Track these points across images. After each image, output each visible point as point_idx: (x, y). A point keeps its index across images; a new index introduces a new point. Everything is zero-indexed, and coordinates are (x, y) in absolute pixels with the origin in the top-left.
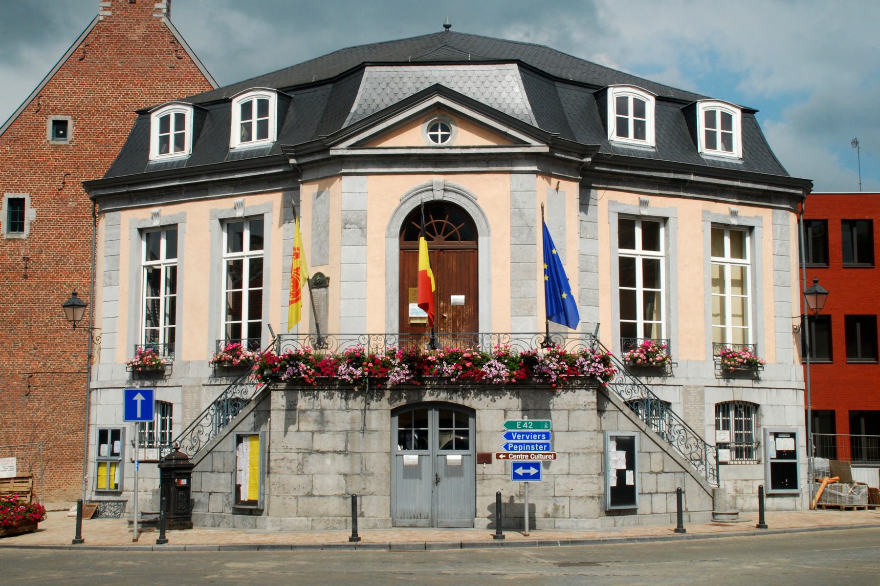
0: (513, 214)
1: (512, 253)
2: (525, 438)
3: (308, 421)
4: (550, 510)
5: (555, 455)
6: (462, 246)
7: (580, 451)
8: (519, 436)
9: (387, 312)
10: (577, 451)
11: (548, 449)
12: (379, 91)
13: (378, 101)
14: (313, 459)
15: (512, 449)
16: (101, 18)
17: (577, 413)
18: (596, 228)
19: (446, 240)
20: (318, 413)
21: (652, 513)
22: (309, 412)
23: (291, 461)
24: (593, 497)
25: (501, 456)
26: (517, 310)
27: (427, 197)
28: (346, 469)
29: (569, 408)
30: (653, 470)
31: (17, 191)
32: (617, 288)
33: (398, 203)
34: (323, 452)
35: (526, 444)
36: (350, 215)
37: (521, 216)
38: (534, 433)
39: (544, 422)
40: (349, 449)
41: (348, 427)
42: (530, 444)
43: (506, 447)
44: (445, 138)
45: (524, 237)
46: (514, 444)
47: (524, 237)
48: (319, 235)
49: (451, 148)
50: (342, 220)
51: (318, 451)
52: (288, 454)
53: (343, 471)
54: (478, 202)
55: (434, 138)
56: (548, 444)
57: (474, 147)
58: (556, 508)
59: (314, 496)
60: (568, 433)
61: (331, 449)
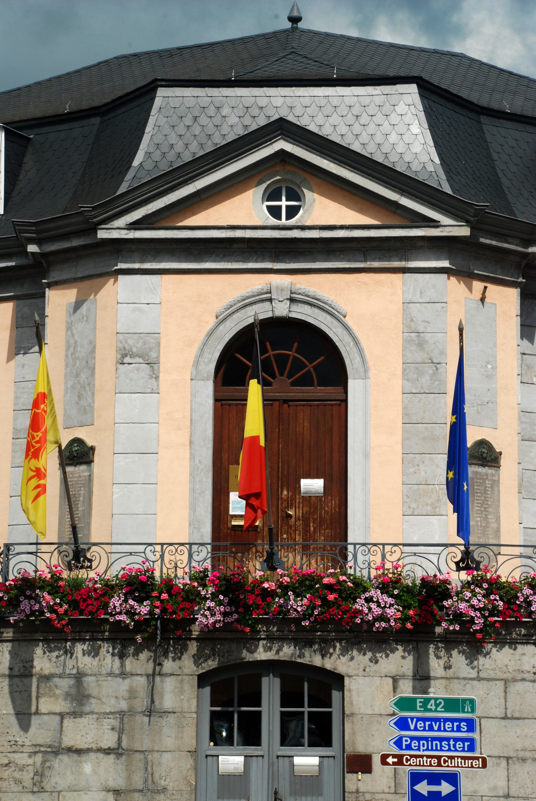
0: (406, 342)
1: (404, 408)
2: (431, 729)
3: (55, 695)
5: (484, 760)
6: (319, 395)
7: (528, 754)
8: (420, 724)
9: (193, 507)
10: (521, 754)
12: (181, 129)
13: (179, 147)
15: (409, 747)
17: (520, 686)
19: (293, 384)
20: (72, 682)
22: (56, 680)
23: (22, 768)
25: (390, 760)
26: (414, 505)
27: (264, 312)
28: (119, 782)
29: (505, 676)
33: (212, 322)
34: (79, 752)
35: (434, 739)
36: (130, 342)
37: (421, 345)
38: (446, 720)
39: (464, 701)
40: (124, 744)
41: (124, 705)
42: (441, 739)
43: (398, 743)
44: (292, 212)
45: (425, 380)
46: (412, 738)
47: (425, 380)
48: (77, 375)
49: (303, 228)
50: (118, 350)
51: (70, 750)
52: (16, 756)
53: (112, 784)
54: (348, 321)
55: (275, 212)
57: (342, 227)
60: (504, 722)
61: (94, 746)
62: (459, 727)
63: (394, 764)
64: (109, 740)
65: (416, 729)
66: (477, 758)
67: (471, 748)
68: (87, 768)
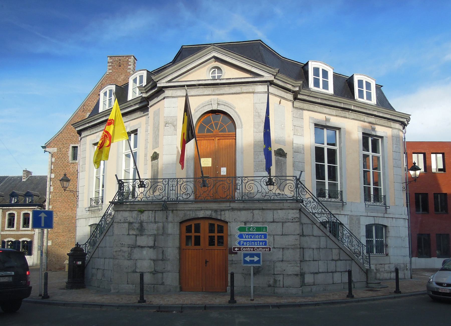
2: (251, 238)
4: (271, 282)
5: (270, 248)
7: (289, 247)
10: (287, 247)
11: (265, 244)
14: (136, 251)
15: (243, 245)
16: (108, 73)
17: (287, 224)
18: (303, 130)
20: (139, 225)
21: (333, 283)
23: (124, 252)
24: (297, 275)
28: (154, 257)
29: (283, 221)
30: (334, 258)
31: (75, 143)
32: (314, 163)
34: (142, 247)
35: (252, 241)
38: (256, 234)
39: (263, 227)
40: (156, 245)
41: (156, 232)
42: (254, 241)
43: (239, 243)
46: (244, 241)
51: (139, 246)
52: (123, 248)
53: (152, 258)
56: (266, 242)
58: (275, 281)
59: (137, 272)
60: (282, 236)
61: (146, 245)
62: (261, 237)
63: (238, 250)
64: (151, 244)
65: (246, 238)
66: (267, 248)
67: (265, 244)
68: (145, 252)
